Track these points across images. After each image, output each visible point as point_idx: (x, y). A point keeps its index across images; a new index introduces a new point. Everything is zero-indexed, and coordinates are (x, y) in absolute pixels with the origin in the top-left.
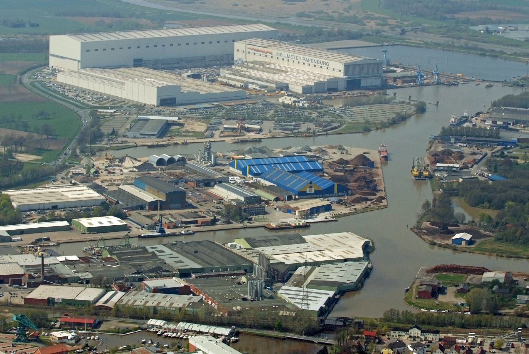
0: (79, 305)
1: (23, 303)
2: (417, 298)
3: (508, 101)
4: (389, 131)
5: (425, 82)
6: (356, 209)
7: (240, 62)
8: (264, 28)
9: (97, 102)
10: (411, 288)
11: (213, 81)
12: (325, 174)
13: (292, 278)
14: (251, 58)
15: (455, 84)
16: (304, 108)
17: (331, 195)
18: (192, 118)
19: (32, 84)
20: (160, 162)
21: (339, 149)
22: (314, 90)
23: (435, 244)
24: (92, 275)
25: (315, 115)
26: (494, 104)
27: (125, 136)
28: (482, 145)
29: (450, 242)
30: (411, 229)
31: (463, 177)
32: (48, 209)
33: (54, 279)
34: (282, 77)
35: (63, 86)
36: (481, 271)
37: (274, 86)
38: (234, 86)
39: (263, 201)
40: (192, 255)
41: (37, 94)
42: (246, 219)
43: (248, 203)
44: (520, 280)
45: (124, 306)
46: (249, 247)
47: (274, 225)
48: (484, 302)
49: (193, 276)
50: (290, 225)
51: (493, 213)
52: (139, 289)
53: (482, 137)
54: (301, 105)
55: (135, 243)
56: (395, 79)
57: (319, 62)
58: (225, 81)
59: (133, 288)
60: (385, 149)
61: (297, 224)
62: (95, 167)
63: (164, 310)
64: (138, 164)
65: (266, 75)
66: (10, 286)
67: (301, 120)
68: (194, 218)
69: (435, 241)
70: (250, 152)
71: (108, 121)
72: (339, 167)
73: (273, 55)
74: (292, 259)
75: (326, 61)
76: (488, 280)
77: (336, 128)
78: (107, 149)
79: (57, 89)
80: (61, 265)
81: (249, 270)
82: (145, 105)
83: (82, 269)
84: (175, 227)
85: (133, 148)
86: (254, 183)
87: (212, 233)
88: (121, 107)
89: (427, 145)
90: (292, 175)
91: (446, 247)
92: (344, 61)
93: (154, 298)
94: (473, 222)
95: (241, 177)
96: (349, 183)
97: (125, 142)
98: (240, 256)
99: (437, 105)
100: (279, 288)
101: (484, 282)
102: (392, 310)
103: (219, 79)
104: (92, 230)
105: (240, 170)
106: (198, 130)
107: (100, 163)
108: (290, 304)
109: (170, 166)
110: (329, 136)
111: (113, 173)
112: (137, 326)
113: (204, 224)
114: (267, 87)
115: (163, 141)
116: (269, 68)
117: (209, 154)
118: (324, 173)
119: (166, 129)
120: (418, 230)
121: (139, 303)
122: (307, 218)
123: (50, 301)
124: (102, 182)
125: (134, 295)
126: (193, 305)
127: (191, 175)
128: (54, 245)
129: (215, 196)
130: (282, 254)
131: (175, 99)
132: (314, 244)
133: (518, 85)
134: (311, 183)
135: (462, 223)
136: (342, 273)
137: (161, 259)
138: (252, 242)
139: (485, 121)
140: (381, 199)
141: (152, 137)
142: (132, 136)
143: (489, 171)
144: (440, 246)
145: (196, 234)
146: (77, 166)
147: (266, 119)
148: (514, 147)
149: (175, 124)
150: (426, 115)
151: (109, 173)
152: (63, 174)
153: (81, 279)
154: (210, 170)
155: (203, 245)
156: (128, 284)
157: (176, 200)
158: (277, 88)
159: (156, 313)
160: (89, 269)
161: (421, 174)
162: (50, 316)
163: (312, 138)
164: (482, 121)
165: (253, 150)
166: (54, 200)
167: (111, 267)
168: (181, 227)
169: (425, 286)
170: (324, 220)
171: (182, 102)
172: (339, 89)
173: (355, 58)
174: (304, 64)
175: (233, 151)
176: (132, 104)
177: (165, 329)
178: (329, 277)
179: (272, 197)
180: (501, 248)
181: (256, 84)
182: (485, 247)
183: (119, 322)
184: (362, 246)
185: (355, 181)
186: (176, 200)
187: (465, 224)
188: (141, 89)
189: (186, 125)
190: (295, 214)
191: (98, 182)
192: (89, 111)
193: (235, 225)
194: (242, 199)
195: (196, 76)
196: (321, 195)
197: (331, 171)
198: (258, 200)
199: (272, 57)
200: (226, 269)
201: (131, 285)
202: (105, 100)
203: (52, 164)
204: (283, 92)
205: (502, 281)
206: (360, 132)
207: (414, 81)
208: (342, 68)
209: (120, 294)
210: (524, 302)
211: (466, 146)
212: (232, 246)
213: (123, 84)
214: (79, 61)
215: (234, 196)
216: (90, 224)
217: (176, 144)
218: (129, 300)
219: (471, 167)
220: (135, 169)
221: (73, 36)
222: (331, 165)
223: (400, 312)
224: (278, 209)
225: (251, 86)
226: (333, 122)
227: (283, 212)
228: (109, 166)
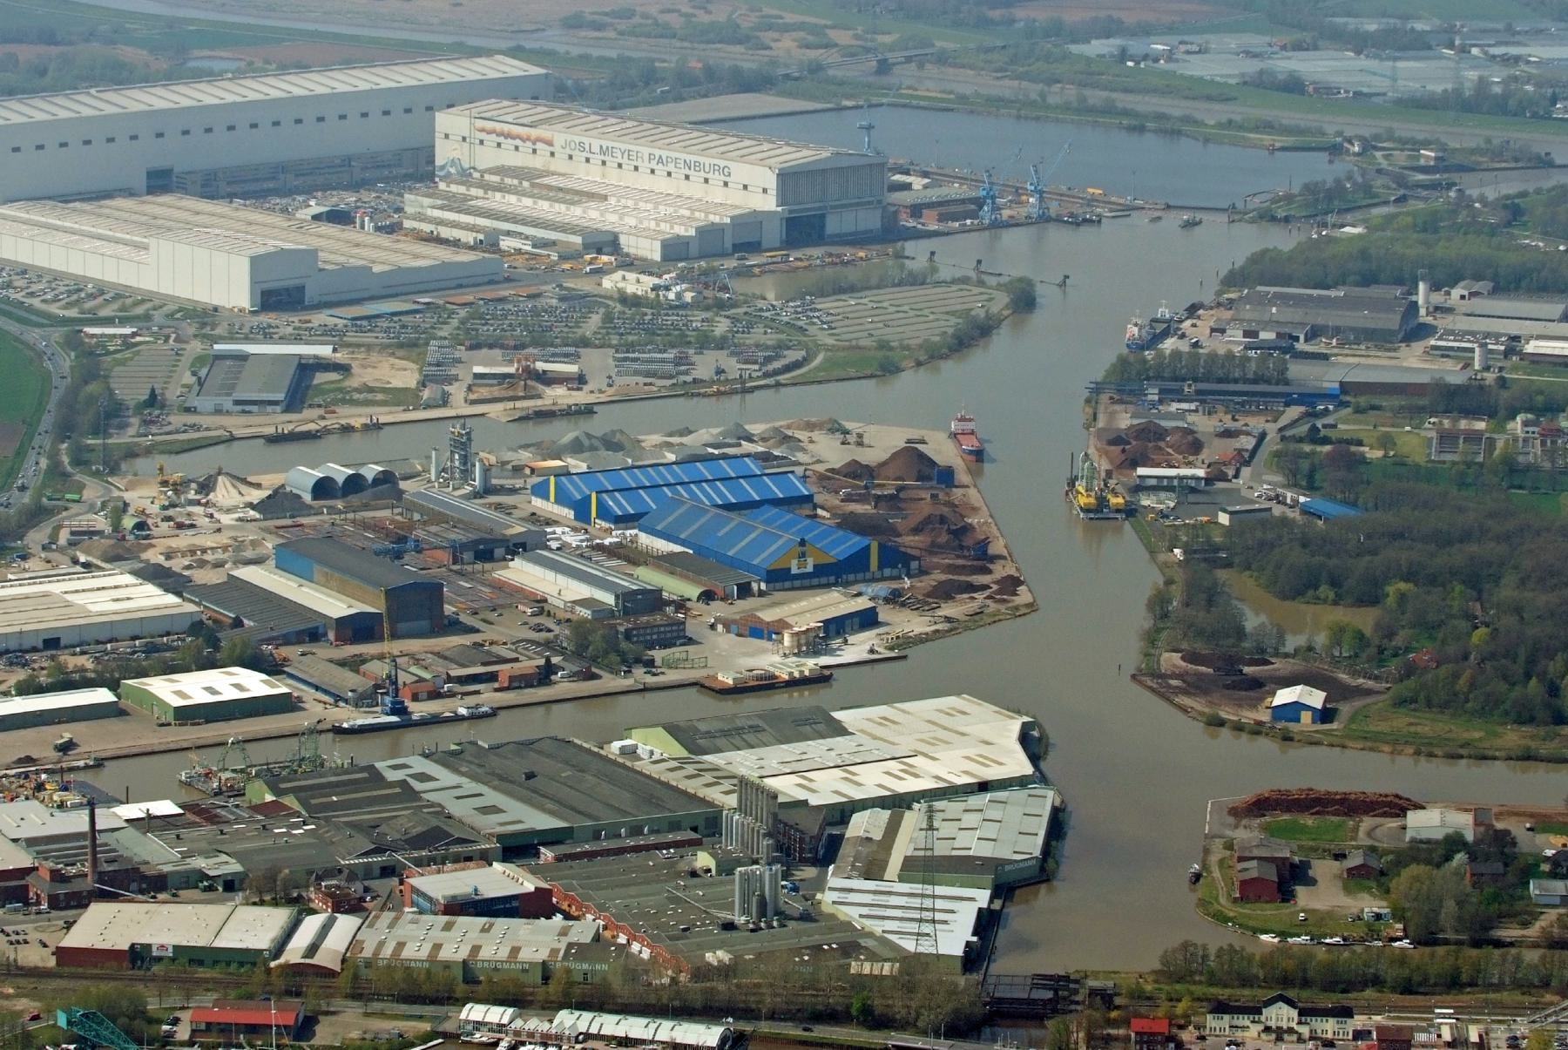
0: (228, 964)
1: (52, 962)
2: (1235, 900)
4: (948, 366)
6: (948, 619)
7: (453, 170)
9: (69, 305)
10: (1205, 866)
11: (392, 229)
12: (820, 512)
13: (846, 851)
14: (488, 157)
15: (1090, 221)
16: (685, 306)
17: (860, 576)
18: (369, 348)
21: (832, 431)
22: (694, 250)
23: (1221, 723)
26: (1233, 279)
27: (188, 410)
28: (1243, 404)
29: (1265, 716)
30: (1134, 677)
31: (1230, 509)
32: (35, 650)
33: (129, 882)
34: (594, 214)
36: (1398, 807)
38: (456, 244)
40: (520, 785)
42: (638, 661)
43: (627, 612)
44: (1518, 828)
45: (368, 964)
46: (684, 753)
47: (727, 679)
48: (1450, 906)
49: (547, 854)
50: (774, 677)
51: (1365, 620)
52: (393, 903)
53: (1236, 381)
54: (671, 296)
55: (337, 755)
58: (426, 228)
59: (373, 898)
61: (797, 675)
62: (131, 510)
63: (496, 969)
64: (256, 496)
65: (544, 209)
68: (484, 664)
69: (1224, 715)
70: (576, 448)
71: (123, 363)
72: (854, 487)
73: (557, 149)
74: (826, 789)
76: (1424, 835)
77: (797, 365)
78: (148, 451)
80: (131, 832)
81: (709, 825)
82: (216, 309)
83: (203, 845)
84: (435, 695)
85: (221, 447)
86: (619, 545)
87: (541, 709)
88: (147, 317)
89: (1080, 413)
91: (1258, 733)
93: (455, 933)
94: (1310, 649)
95: (574, 529)
96: (899, 535)
97: (195, 427)
98: (667, 785)
99: (1063, 284)
100: (820, 884)
101: (1413, 840)
102: (1185, 946)
103: (408, 224)
104: (189, 715)
107: (144, 497)
108: (871, 935)
109: (355, 499)
110: (783, 390)
111: (192, 526)
112: (426, 1027)
115: (307, 420)
116: (549, 188)
117: (465, 459)
118: (815, 507)
120: (1150, 677)
121: (416, 951)
123: (138, 955)
125: (391, 926)
126: (578, 951)
127: (433, 529)
128: (87, 767)
129: (517, 594)
130: (805, 775)
132: (875, 738)
134: (803, 543)
135: (1277, 655)
136: (991, 830)
137: (433, 805)
138: (693, 740)
139: (1223, 331)
140: (1011, 584)
141: (269, 409)
143: (1293, 485)
144: (1239, 728)
146: (75, 508)
147: (585, 343)
148: (1335, 411)
149: (322, 365)
150: (1038, 319)
151: (180, 526)
153: (208, 877)
154: (476, 507)
155: (540, 752)
156: (356, 888)
158: (587, 247)
159: (471, 982)
160: (223, 842)
161: (1102, 502)
162: (153, 1006)
163: (737, 398)
164: (1213, 330)
165: (586, 443)
166: (49, 621)
167: (287, 834)
168: (451, 694)
169: (1254, 863)
170: (866, 656)
172: (765, 245)
173: (805, 153)
174: (653, 171)
175: (525, 447)
177: (517, 1033)
178: (957, 844)
179: (693, 591)
180: (1419, 729)
182: (1372, 728)
183: (367, 1015)
185: (916, 530)
187: (1286, 655)
188: (199, 262)
189: (356, 370)
190: (781, 642)
191: (154, 556)
192: (57, 334)
194: (608, 599)
195: (338, 217)
196: (832, 579)
197: (834, 501)
198: (653, 600)
199: (552, 154)
200: (636, 831)
201: (367, 890)
202: (92, 296)
204: (605, 258)
206: (872, 376)
209: (346, 924)
210: (1557, 901)
211: (1196, 411)
212: (624, 751)
215: (578, 590)
216: (180, 694)
217: (347, 429)
218: (381, 944)
219: (1236, 476)
220: (252, 513)
222: (827, 480)
223: (1212, 951)
224: (720, 627)
225: (506, 244)
226: (781, 347)
227: (739, 635)
228: (173, 505)
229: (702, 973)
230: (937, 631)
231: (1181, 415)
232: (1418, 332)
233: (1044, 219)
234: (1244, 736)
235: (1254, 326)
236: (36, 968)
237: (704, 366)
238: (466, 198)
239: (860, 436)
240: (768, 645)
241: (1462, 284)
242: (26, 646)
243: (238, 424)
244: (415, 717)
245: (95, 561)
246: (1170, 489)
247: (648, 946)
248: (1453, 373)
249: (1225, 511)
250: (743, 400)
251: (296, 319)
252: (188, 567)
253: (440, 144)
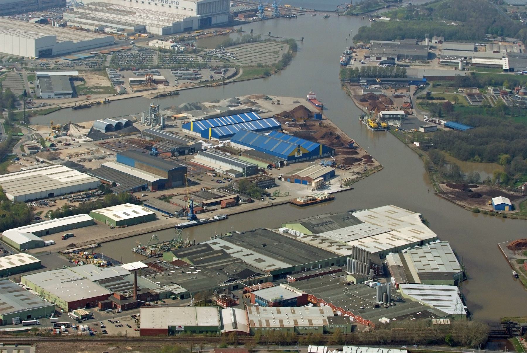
1: (138, 334)
6: (358, 173)
11: (64, 25)
16: (181, 52)
17: (316, 157)
22: (172, 32)
23: (479, 212)
24: (183, 287)
26: (357, 38)
27: (39, 98)
31: (424, 126)
32: (46, 198)
38: (88, 30)
39: (259, 170)
40: (262, 249)
42: (264, 194)
46: (311, 233)
50: (316, 199)
58: (76, 25)
59: (237, 299)
61: (323, 198)
63: (306, 329)
66: (101, 310)
68: (214, 198)
85: (57, 112)
90: (259, 134)
104: (122, 224)
105: (199, 133)
107: (46, 133)
110: (235, 83)
115: (81, 101)
116: (114, 10)
118: (282, 130)
127: (160, 143)
128: (95, 247)
131: (51, 49)
133: (353, 15)
134: (299, 146)
135: (478, 183)
139: (369, 57)
141: (67, 96)
142: (47, 96)
151: (66, 145)
153: (174, 294)
157: (178, 177)
158: (136, 30)
161: (379, 124)
163: (222, 87)
165: (189, 107)
171: (59, 53)
172: (194, 28)
174: (149, 3)
175: (168, 109)
176: (8, 57)
179: (265, 165)
181: (110, 27)
190: (311, 185)
194: (241, 170)
195: (43, 22)
196: (308, 158)
200: (315, 266)
201: (234, 296)
212: (284, 232)
217: (99, 103)
220: (88, 138)
224: (283, 179)
225: (107, 30)
229: (379, 325)
230: (357, 178)
231: (377, 90)
232: (431, 56)
233: (278, 16)
234: (488, 216)
235: (379, 56)
236: (133, 337)
237: (206, 75)
238: (86, 14)
239: (279, 101)
241: (434, 38)
242: (43, 197)
244: (201, 221)
245: (45, 160)
246: (398, 119)
247: (352, 316)
248: (450, 72)
249: (423, 127)
250: (224, 87)
251: (54, 61)
252: (80, 161)
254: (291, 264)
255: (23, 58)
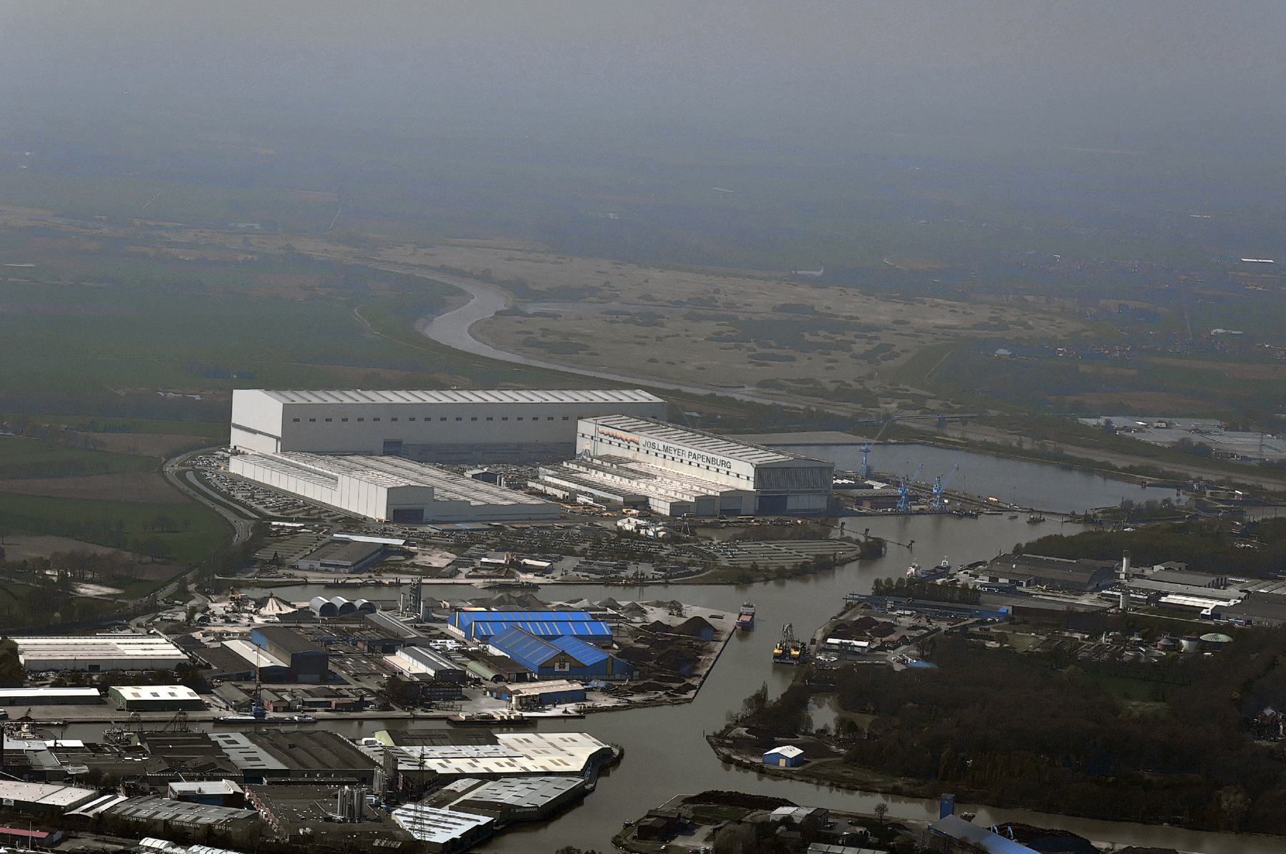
3: (1050, 545)
5: (916, 508)
8: (643, 397)
14: (604, 449)
19: (181, 475)
20: (328, 609)
25: (669, 549)
27: (293, 567)
35: (235, 479)
37: (621, 499)
38: (554, 498)
39: (470, 679)
41: (180, 490)
47: (462, 717)
54: (651, 534)
56: (859, 501)
57: (713, 461)
60: (751, 610)
67: (633, 559)
73: (641, 446)
75: (727, 460)
77: (691, 573)
79: (220, 485)
84: (289, 708)
92: (756, 461)
97: (290, 576)
103: (530, 484)
106: (435, 564)
113: (339, 708)
114: (609, 500)
116: (628, 469)
119: (380, 559)
122: (532, 710)
124: (205, 635)
144: (739, 765)
145: (320, 724)
152: (142, 620)
155: (314, 739)
179: (490, 675)
181: (592, 495)
184: (592, 758)
186: (308, 665)
188: (362, 492)
193: (398, 713)
194: (432, 673)
195: (489, 478)
198: (462, 678)
203: (131, 604)
204: (634, 511)
205: (797, 821)
206: (731, 584)
207: (893, 505)
208: (752, 474)
213: (336, 479)
214: (278, 439)
217: (379, 585)
221: (273, 393)
228: (234, 611)
238: (574, 471)
240: (504, 703)
243: (313, 577)
253: (579, 440)
254: (285, 764)
255: (365, 518)
